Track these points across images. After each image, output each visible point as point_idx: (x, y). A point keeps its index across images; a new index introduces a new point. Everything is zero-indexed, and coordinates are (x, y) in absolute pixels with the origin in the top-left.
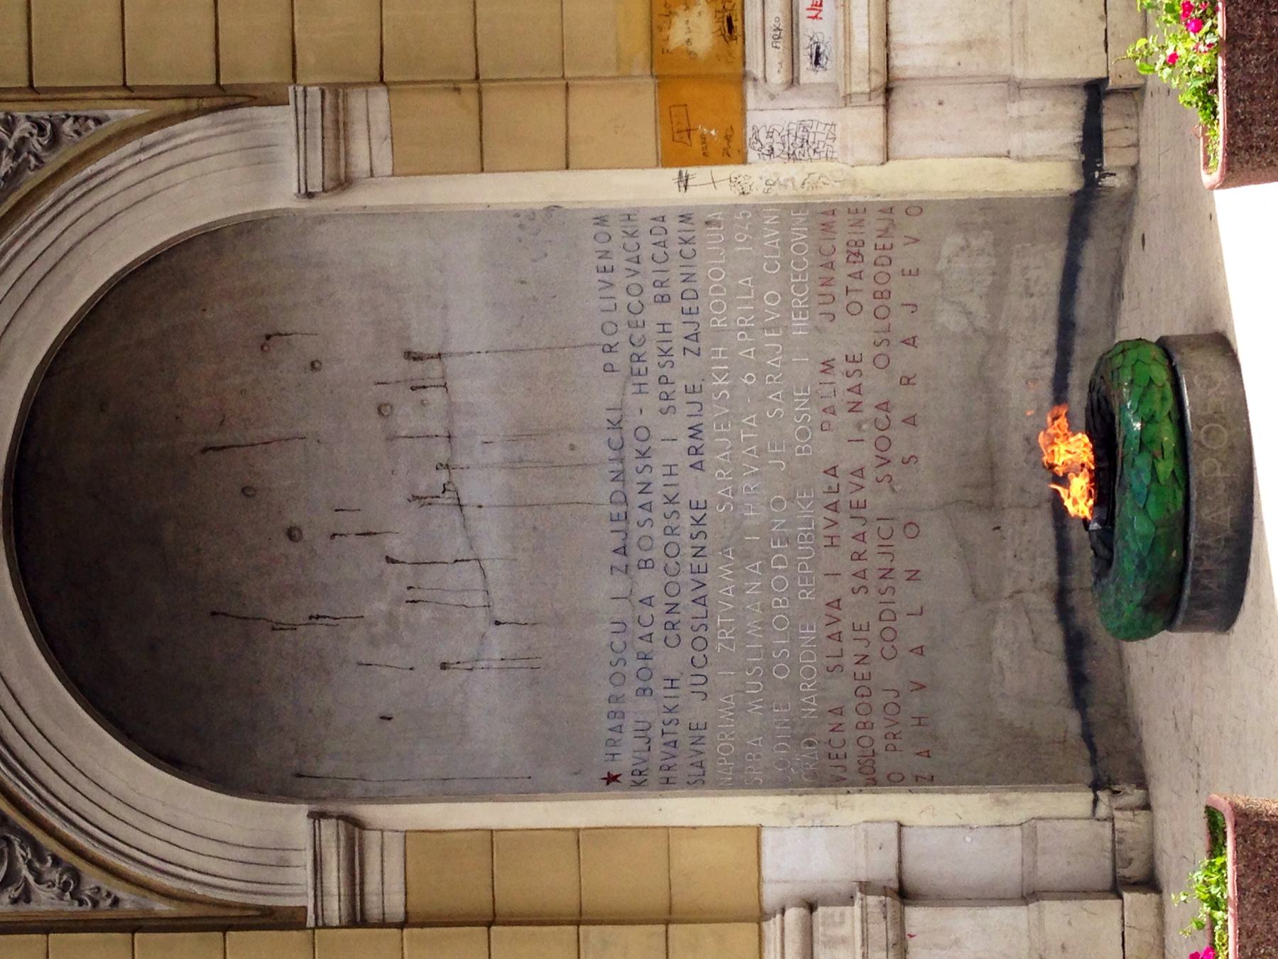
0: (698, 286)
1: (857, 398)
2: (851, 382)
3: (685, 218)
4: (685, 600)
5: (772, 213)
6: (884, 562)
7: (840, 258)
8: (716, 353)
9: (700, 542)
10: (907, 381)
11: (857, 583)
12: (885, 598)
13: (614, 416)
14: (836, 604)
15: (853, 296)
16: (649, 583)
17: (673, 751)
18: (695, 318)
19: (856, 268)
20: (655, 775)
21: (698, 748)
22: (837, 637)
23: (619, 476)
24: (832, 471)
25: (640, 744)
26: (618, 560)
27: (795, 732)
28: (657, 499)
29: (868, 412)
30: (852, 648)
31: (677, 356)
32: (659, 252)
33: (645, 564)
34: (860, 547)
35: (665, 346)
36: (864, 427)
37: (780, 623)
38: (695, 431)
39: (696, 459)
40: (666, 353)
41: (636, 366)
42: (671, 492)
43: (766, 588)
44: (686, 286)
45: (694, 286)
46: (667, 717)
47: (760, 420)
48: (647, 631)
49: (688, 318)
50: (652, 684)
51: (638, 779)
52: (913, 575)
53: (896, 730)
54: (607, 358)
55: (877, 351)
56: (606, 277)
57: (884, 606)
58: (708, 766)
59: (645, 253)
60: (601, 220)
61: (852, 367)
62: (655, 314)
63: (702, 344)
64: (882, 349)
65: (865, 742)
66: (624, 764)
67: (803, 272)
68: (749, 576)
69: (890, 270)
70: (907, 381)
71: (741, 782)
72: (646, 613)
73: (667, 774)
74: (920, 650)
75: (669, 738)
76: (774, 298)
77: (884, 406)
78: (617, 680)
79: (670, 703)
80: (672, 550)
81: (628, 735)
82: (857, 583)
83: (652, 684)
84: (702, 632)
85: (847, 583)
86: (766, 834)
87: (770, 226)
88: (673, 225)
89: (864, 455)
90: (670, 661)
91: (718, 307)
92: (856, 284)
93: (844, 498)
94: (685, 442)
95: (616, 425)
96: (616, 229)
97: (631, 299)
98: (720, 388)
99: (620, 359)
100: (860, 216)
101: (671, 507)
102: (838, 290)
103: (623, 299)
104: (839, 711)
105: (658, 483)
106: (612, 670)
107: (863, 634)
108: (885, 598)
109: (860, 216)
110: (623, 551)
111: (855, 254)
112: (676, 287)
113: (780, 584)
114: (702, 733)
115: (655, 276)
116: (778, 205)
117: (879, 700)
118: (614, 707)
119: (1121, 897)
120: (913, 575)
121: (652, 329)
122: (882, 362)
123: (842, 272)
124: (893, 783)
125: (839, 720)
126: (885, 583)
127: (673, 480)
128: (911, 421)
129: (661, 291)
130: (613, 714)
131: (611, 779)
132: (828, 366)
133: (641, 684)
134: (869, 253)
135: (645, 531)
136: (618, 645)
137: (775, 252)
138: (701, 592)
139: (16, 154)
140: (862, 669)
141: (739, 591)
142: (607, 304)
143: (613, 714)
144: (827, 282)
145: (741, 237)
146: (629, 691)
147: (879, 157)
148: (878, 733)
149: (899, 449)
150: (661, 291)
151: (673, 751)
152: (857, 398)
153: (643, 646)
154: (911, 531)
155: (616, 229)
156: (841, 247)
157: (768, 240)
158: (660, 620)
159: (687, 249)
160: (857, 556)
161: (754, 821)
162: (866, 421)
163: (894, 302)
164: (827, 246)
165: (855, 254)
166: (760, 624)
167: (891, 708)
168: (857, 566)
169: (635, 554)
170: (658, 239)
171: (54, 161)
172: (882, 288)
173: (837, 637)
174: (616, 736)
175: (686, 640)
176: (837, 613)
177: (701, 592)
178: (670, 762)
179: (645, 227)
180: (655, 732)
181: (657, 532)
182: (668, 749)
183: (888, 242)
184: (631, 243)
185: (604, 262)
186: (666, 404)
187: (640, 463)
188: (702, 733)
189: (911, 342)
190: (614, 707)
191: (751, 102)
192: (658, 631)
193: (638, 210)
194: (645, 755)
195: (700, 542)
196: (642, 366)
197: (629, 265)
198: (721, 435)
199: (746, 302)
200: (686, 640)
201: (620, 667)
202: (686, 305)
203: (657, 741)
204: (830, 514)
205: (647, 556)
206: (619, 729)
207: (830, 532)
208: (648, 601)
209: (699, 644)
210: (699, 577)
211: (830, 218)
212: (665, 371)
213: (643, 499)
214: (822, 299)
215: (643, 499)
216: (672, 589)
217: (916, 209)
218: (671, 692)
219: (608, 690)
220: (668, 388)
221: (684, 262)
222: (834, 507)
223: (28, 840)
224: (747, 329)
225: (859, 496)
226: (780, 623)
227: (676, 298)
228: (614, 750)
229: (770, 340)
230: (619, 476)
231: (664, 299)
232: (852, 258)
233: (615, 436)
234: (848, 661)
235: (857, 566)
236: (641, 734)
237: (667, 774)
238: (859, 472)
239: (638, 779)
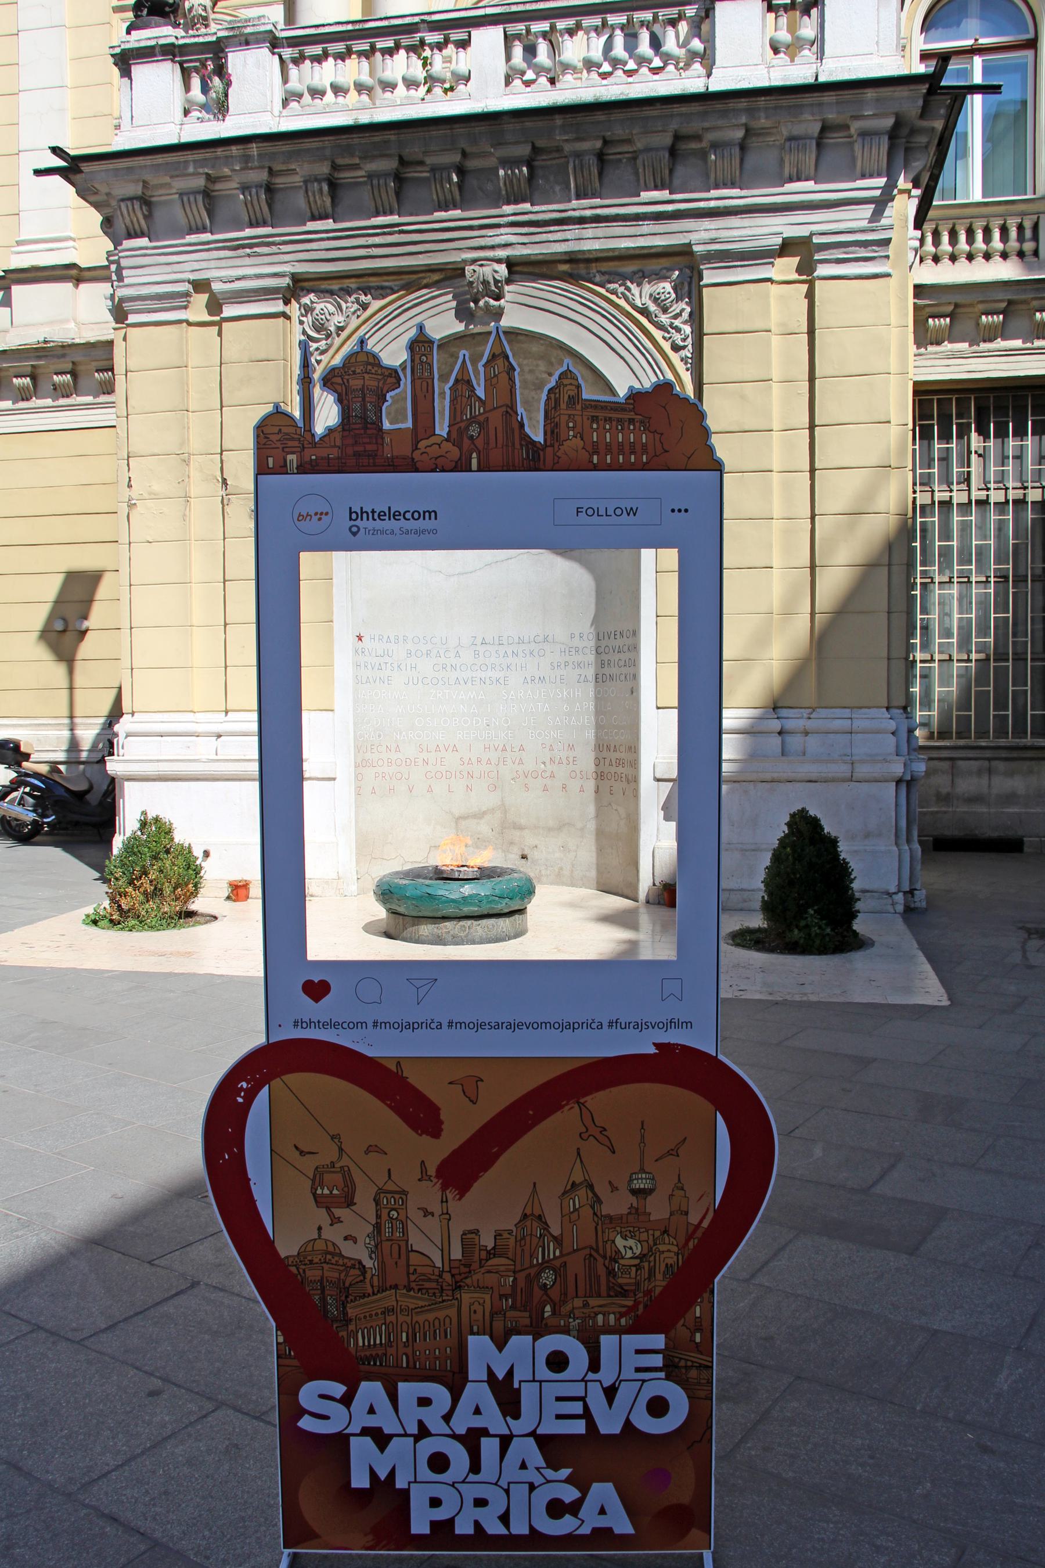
7: (617, 755)
9: (488, 682)
12: (458, 773)
13: (550, 639)
14: (455, 749)
15: (602, 761)
23: (521, 641)
24: (522, 749)
25: (380, 652)
26: (479, 641)
29: (549, 767)
31: (578, 671)
32: (622, 663)
33: (476, 654)
34: (484, 762)
42: (513, 668)
46: (395, 665)
48: (442, 655)
51: (360, 651)
52: (469, 788)
59: (622, 656)
61: (571, 760)
65: (380, 763)
73: (363, 665)
74: (430, 790)
75: (383, 667)
77: (552, 776)
78: (416, 640)
79: (403, 667)
80: (484, 668)
84: (441, 682)
92: (607, 763)
98: (562, 693)
101: (505, 668)
104: (398, 749)
108: (458, 773)
112: (607, 671)
118: (401, 639)
123: (614, 756)
125: (393, 749)
126: (466, 775)
128: (545, 789)
131: (360, 638)
132: (571, 747)
134: (620, 770)
139: (671, 325)
140: (420, 763)
144: (608, 748)
147: (658, 776)
156: (623, 755)
159: (623, 677)
160: (479, 761)
161: (336, 708)
165: (620, 762)
167: (399, 776)
168: (474, 760)
169: (482, 649)
171: (666, 346)
173: (438, 749)
174: (385, 640)
176: (451, 749)
177: (462, 682)
178: (369, 666)
183: (624, 779)
187: (527, 652)
190: (401, 639)
195: (488, 682)
198: (540, 693)
201: (422, 640)
202: (600, 676)
204: (500, 748)
209: (435, 681)
210: (470, 681)
213: (510, 653)
215: (510, 653)
217: (636, 795)
218: (409, 668)
220: (563, 666)
222: (504, 750)
223: (329, 347)
225: (509, 761)
228: (377, 638)
230: (521, 641)
233: (541, 639)
235: (474, 760)
237: (363, 665)
238: (521, 762)
239: (360, 651)
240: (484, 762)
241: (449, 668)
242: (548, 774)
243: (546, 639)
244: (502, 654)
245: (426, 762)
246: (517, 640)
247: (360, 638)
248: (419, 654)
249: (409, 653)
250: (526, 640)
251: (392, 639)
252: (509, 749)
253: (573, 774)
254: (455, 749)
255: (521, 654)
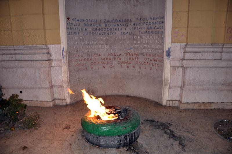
0: (150, 34)
1: (132, 59)
2: (134, 58)
3: (163, 32)
4: (100, 31)
5: (162, 47)
6: (106, 63)
7: (154, 58)
8: (139, 37)
10: (134, 67)
11: (103, 58)
12: (101, 63)
13: (129, 20)
14: (100, 55)
16: (103, 25)
17: (74, 29)
18: (145, 33)
19: (152, 60)
20: (69, 26)
21: (75, 34)
22: (94, 55)
24: (120, 55)
25: (75, 24)
26: (107, 21)
27: (78, 49)
28: (116, 27)
29: (129, 61)
30: (93, 58)
32: (157, 28)
33: (106, 25)
34: (109, 59)
35: (140, 29)
36: (127, 60)
37: (97, 47)
38: (127, 33)
39: (123, 34)
40: (139, 29)
41: (137, 24)
42: (117, 29)
43: (102, 44)
44: (150, 32)
45: (150, 33)
46: (80, 29)
47: (128, 44)
49: (145, 32)
50: (86, 26)
53: (79, 65)
54: (139, 18)
55: (139, 62)
56: (153, 19)
57: (99, 63)
58: (72, 35)
59: (157, 25)
60: (163, 17)
61: (136, 58)
62: (146, 27)
63: (141, 35)
64: (139, 63)
66: (71, 21)
67: (152, 51)
68: (104, 42)
69: (152, 65)
70: (134, 67)
71: (68, 41)
72: (98, 25)
73: (70, 28)
74: (92, 68)
75: (77, 29)
76: (148, 46)
77: (130, 63)
79: (83, 29)
80: (108, 29)
81: (77, 22)
82: (103, 58)
83: (86, 26)
84: (95, 34)
85: (103, 57)
86: (59, 45)
87: (160, 46)
88: (162, 30)
89: (123, 60)
90: (90, 29)
91: (147, 37)
92: (150, 60)
93: (116, 57)
94: (125, 32)
95: (128, 20)
96: (161, 20)
97: (149, 23)
98: (134, 37)
99: (138, 21)
100: (161, 61)
101: (115, 29)
102: (149, 57)
103: (148, 21)
104: (82, 56)
105: (119, 27)
106: (88, 20)
107: (95, 59)
109: (161, 61)
110: (108, 21)
111: (155, 60)
112: (150, 30)
113: (103, 46)
114: (78, 34)
115: (152, 27)
116: (164, 48)
117: (84, 62)
118: (82, 20)
119: (52, 101)
120: (104, 67)
121: (144, 26)
122: (137, 63)
123: (151, 57)
124: (69, 66)
127: (119, 30)
128: (128, 67)
129: (150, 28)
130: (81, 20)
131: (68, 19)
133: (86, 24)
134: (155, 62)
135: (111, 25)
136: (92, 21)
137: (156, 47)
138: (101, 34)
141: (102, 40)
142: (148, 19)
143: (81, 20)
144: (150, 55)
145: (158, 41)
146: (85, 22)
148: (79, 62)
149: (124, 65)
150: (150, 28)
151: (74, 29)
152: (132, 59)
153: (92, 25)
154: (111, 67)
155: (161, 20)
157: (158, 46)
158: (97, 28)
159: (157, 32)
160: (107, 59)
162: (128, 60)
163: (146, 66)
164: (156, 56)
165: (155, 60)
166: (96, 43)
167: (82, 64)
168: (106, 58)
169: (108, 23)
170: (159, 27)
172: (149, 64)
174: (77, 20)
175: (94, 32)
176: (98, 55)
177: (101, 34)
178: (72, 29)
179: (161, 25)
180: (77, 26)
181: (111, 27)
182: (75, 29)
184: (158, 23)
185: (155, 18)
186: (131, 28)
188: (78, 34)
189: (140, 68)
190: (82, 20)
191: (182, 44)
192: (95, 27)
193: (164, 24)
194: (73, 25)
196: (137, 25)
197: (154, 23)
199: (147, 42)
200: (94, 32)
203: (76, 27)
204: (114, 54)
205: (107, 25)
206: (78, 21)
207: (111, 54)
208: (100, 26)
210: (104, 34)
211: (161, 57)
212: (137, 28)
214: (147, 54)
216: (102, 30)
217: (162, 70)
218: (85, 30)
219: (85, 19)
220: (134, 29)
221: (154, 32)
222: (115, 55)
224: (143, 42)
226: (97, 47)
227: (148, 31)
229: (141, 46)
231: (148, 28)
232: (154, 60)
234: (91, 57)
235: (106, 58)
236: (77, 24)
237: (70, 28)
238: (120, 59)
240: (109, 59)
241: (97, 30)
242: (129, 63)
243: (128, 20)
244: (114, 25)
245: (91, 59)
246: (118, 20)
247: (68, 19)
248: (88, 25)
249: (85, 25)
250: (122, 20)
251: (79, 20)
252: (116, 54)
253: (137, 63)
254: (100, 55)
255: (120, 25)
